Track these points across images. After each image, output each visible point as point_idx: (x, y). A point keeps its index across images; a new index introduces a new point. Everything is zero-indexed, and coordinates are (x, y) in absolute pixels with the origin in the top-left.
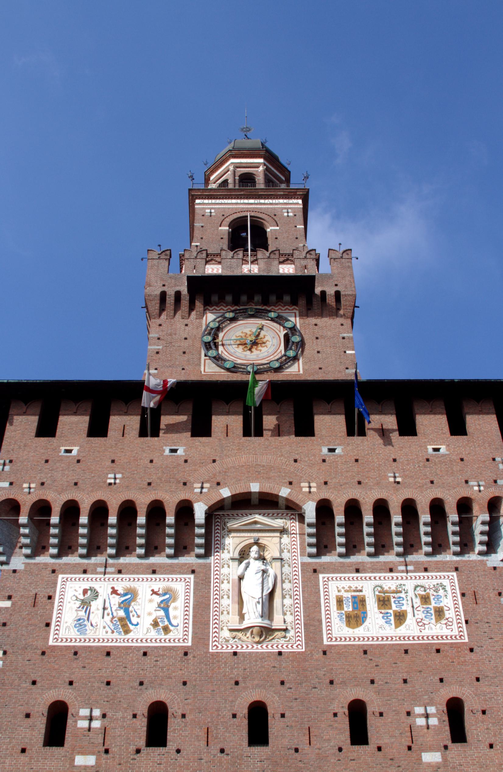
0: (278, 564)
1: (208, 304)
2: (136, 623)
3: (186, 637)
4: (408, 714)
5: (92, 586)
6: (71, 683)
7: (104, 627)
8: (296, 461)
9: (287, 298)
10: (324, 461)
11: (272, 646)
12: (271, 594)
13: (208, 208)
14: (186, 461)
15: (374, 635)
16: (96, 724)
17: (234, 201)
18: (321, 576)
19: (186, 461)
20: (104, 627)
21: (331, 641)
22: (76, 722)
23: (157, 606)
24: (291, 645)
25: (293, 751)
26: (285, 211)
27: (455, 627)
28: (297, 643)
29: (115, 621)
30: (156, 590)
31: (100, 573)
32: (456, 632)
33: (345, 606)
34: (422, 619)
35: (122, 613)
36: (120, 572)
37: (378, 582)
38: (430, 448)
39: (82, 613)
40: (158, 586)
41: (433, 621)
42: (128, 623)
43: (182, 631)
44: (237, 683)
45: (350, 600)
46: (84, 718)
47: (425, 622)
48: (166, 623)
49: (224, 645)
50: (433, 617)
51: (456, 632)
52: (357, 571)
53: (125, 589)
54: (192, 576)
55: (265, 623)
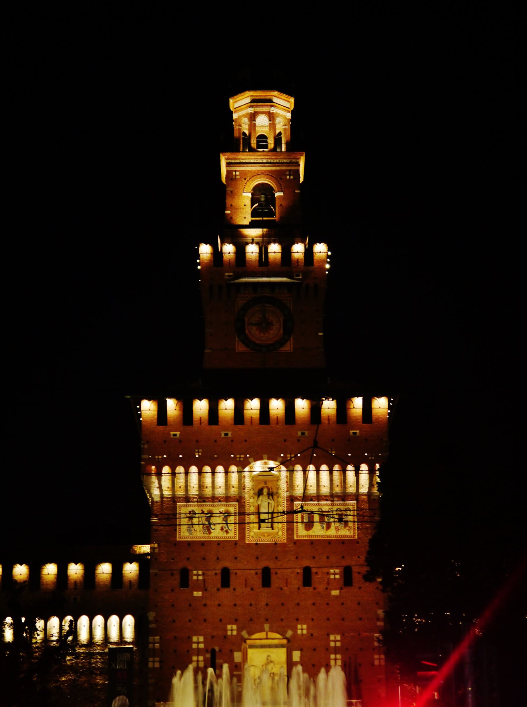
2: (213, 528)
3: (235, 535)
4: (328, 573)
5: (193, 509)
7: (200, 531)
8: (285, 440)
10: (299, 440)
11: (272, 540)
14: (232, 441)
15: (317, 534)
16: (201, 578)
18: (295, 502)
19: (232, 441)
20: (200, 531)
21: (298, 538)
22: (192, 577)
23: (222, 520)
24: (280, 539)
25: (279, 590)
26: (287, 173)
27: (352, 531)
28: (284, 538)
29: (205, 528)
30: (221, 511)
31: (196, 502)
32: (352, 534)
33: (305, 519)
34: (338, 527)
37: (320, 507)
40: (222, 509)
41: (343, 528)
42: (210, 528)
43: (233, 533)
44: (257, 558)
45: (307, 516)
46: (195, 575)
47: (339, 528)
48: (227, 528)
49: (252, 540)
50: (343, 526)
51: (352, 534)
53: (208, 511)
54: (237, 503)
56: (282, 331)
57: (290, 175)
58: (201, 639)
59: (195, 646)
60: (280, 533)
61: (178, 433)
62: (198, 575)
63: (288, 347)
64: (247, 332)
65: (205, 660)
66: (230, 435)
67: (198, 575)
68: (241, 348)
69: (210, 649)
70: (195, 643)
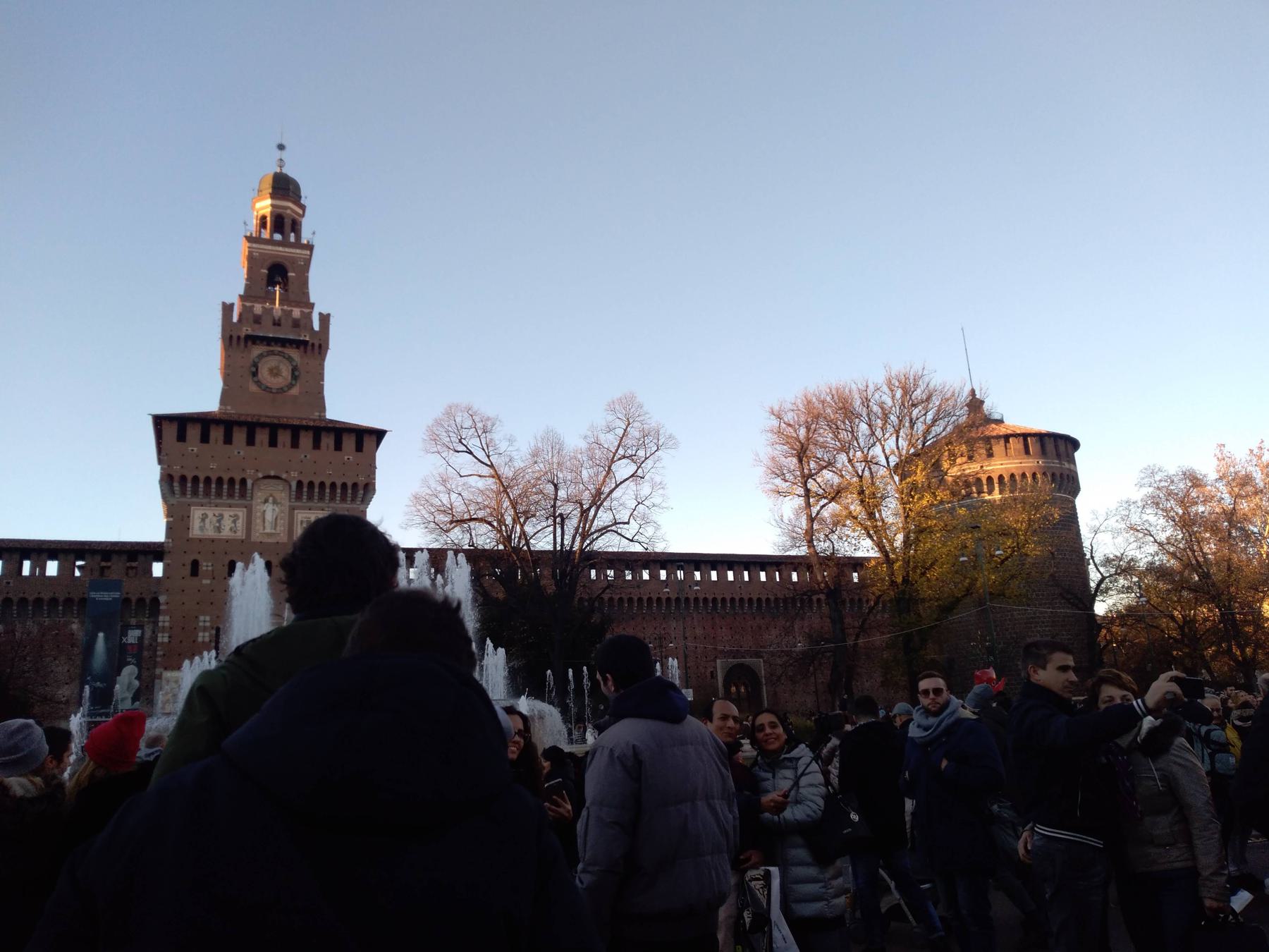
0: (279, 505)
1: (254, 343)
6: (199, 553)
9: (294, 346)
12: (276, 519)
13: (254, 252)
14: (244, 458)
16: (210, 568)
17: (270, 247)
35: (217, 525)
36: (216, 506)
38: (346, 457)
39: (202, 524)
40: (232, 513)
52: (310, 510)
54: (245, 510)
55: (273, 531)
56: (290, 377)
57: (301, 261)
58: (208, 618)
59: (201, 624)
60: (282, 535)
61: (195, 449)
62: (207, 566)
63: (295, 391)
64: (260, 375)
65: (211, 636)
66: (242, 453)
67: (207, 566)
68: (253, 388)
69: (215, 626)
70: (201, 621)
